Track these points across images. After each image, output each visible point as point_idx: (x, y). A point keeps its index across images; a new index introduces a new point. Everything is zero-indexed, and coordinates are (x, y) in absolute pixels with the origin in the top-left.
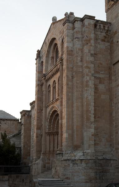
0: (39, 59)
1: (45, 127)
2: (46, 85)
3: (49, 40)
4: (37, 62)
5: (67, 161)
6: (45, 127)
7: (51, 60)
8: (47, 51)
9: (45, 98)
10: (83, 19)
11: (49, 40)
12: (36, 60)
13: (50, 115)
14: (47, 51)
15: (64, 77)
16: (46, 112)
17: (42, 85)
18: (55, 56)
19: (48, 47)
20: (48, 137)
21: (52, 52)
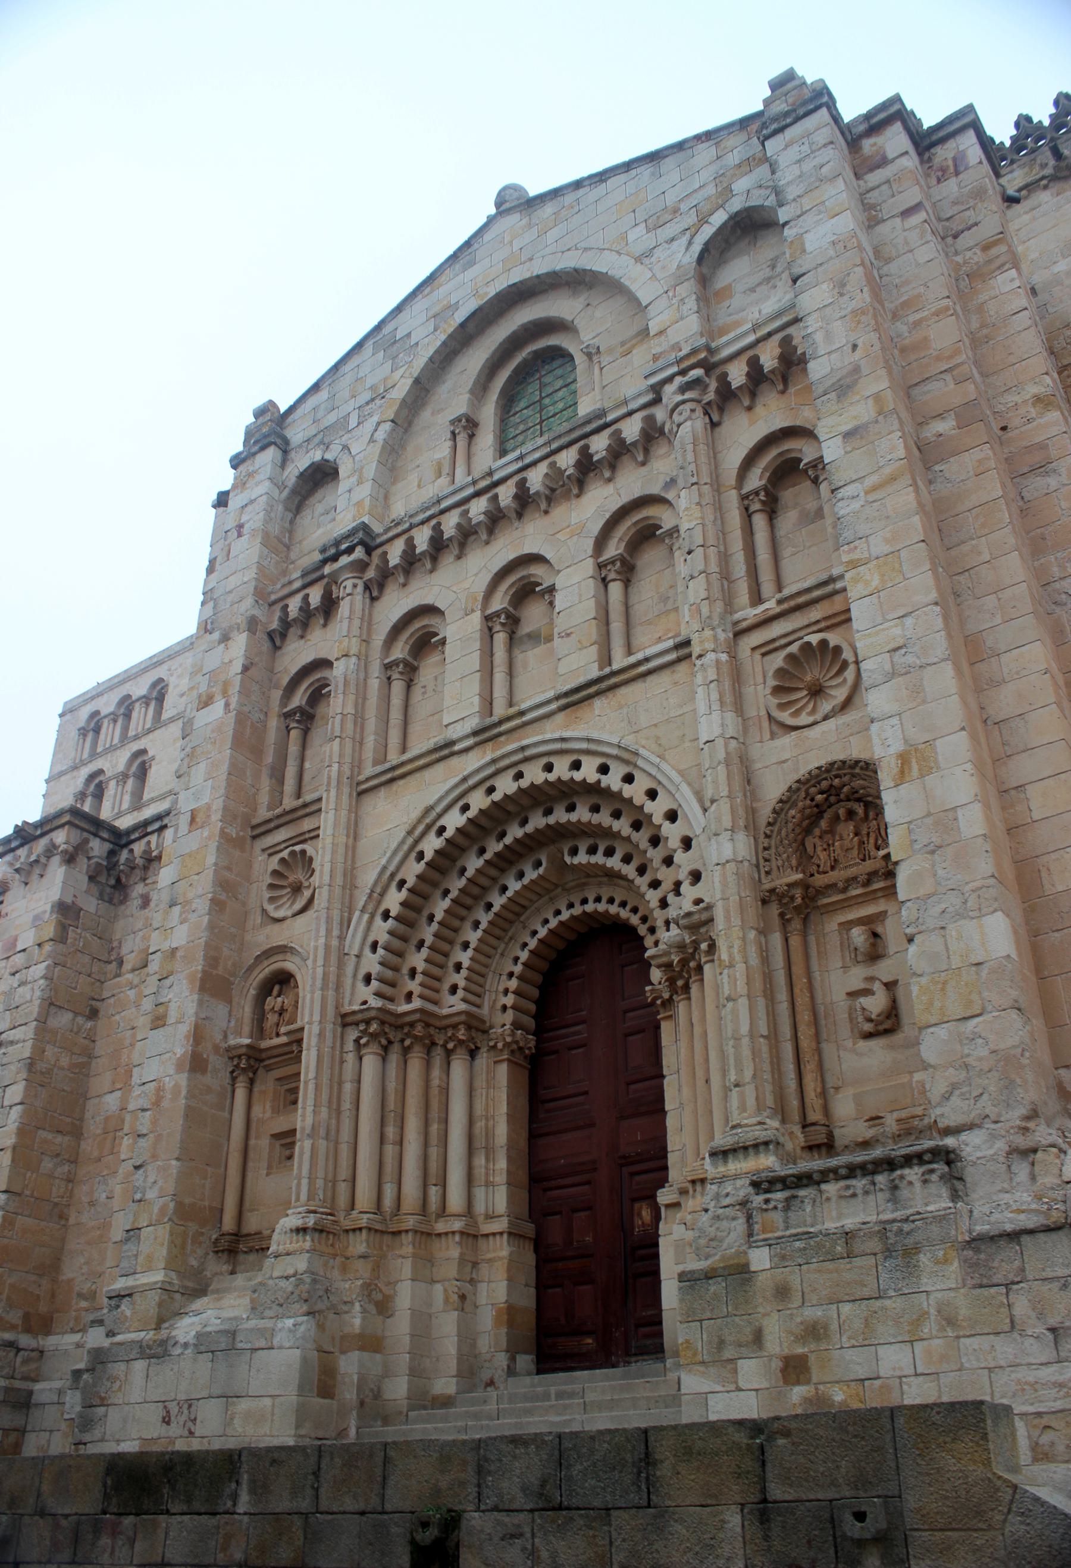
0: (279, 454)
1: (341, 965)
2: (368, 622)
3: (456, 307)
4: (240, 484)
5: (1025, 1239)
6: (341, 965)
7: (454, 434)
8: (409, 382)
9: (350, 709)
10: (935, 137)
11: (455, 307)
12: (235, 467)
13: (432, 845)
14: (417, 381)
15: (847, 435)
16: (354, 831)
17: (284, 636)
18: (488, 414)
19: (436, 352)
20: (370, 1063)
21: (472, 392)
